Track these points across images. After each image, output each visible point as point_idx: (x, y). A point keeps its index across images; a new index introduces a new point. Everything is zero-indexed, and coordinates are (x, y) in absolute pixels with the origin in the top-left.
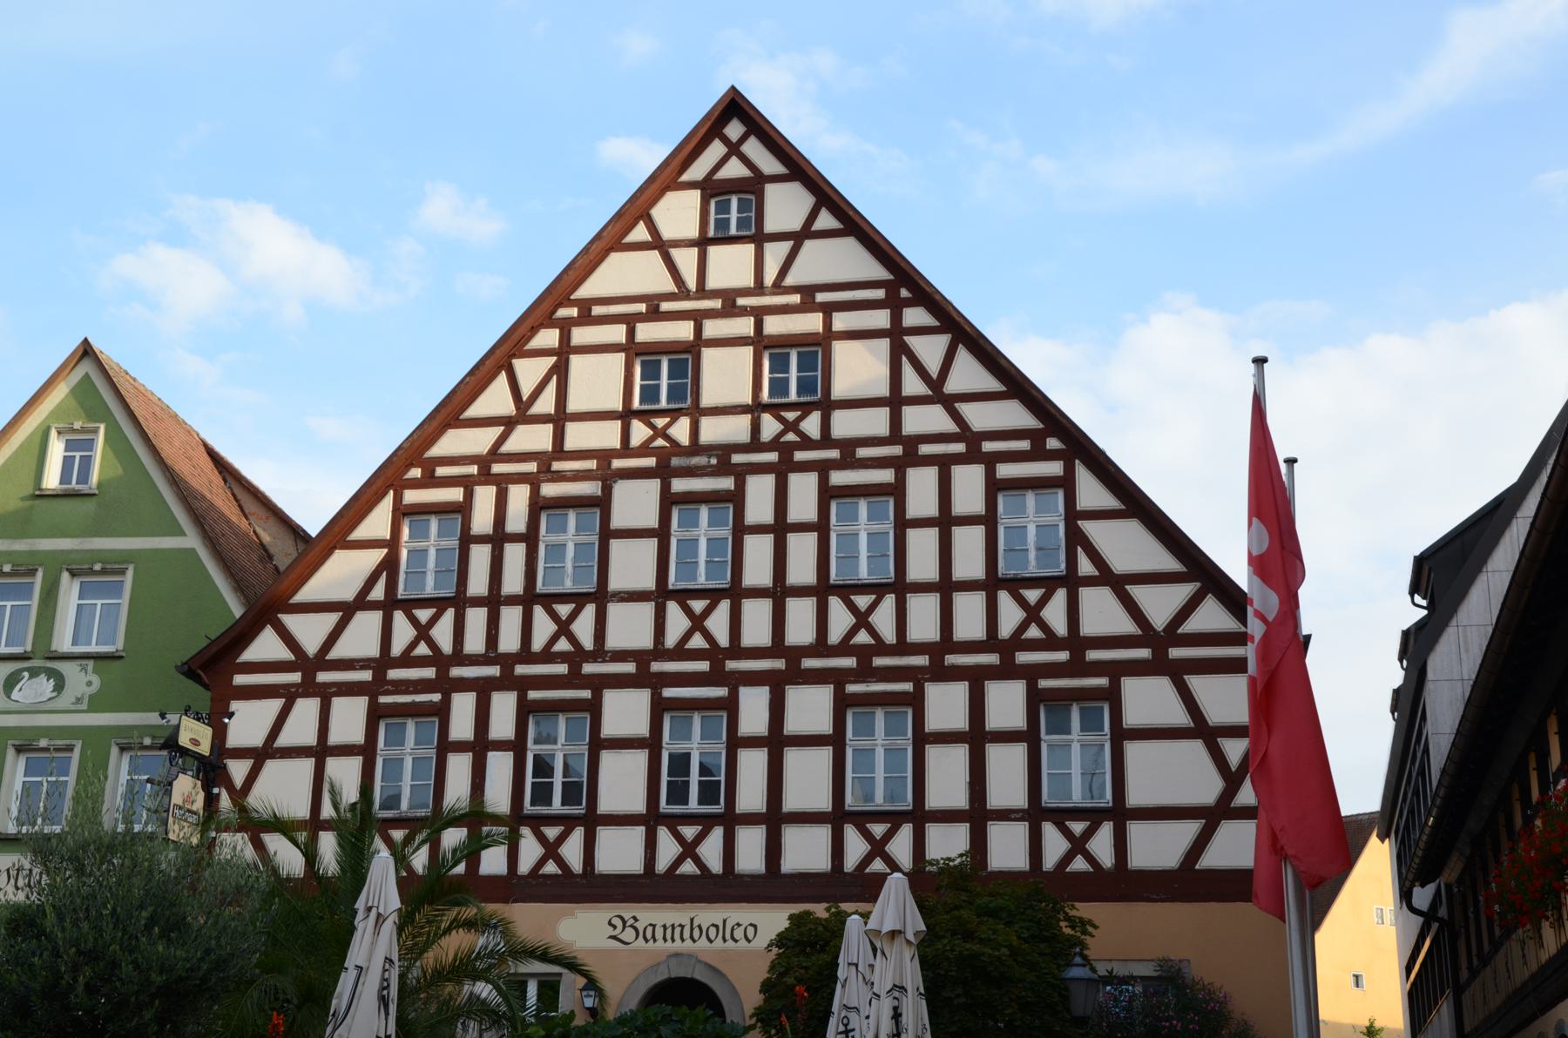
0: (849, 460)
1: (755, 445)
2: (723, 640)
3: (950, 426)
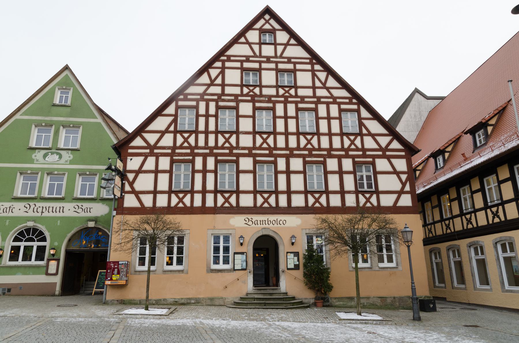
0: (303, 102)
1: (277, 96)
2: (272, 145)
3: (328, 95)
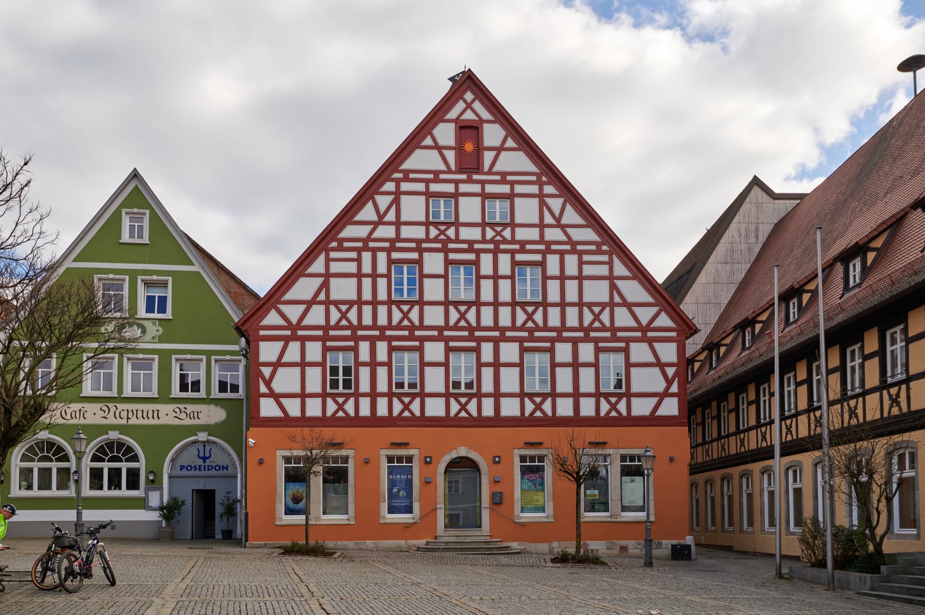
0: (523, 251)
1: (484, 241)
2: (474, 323)
3: (563, 238)
